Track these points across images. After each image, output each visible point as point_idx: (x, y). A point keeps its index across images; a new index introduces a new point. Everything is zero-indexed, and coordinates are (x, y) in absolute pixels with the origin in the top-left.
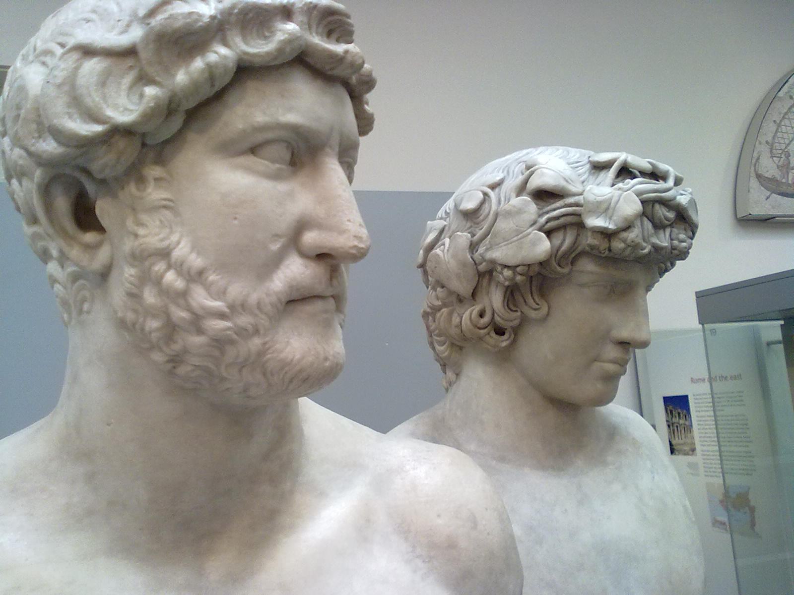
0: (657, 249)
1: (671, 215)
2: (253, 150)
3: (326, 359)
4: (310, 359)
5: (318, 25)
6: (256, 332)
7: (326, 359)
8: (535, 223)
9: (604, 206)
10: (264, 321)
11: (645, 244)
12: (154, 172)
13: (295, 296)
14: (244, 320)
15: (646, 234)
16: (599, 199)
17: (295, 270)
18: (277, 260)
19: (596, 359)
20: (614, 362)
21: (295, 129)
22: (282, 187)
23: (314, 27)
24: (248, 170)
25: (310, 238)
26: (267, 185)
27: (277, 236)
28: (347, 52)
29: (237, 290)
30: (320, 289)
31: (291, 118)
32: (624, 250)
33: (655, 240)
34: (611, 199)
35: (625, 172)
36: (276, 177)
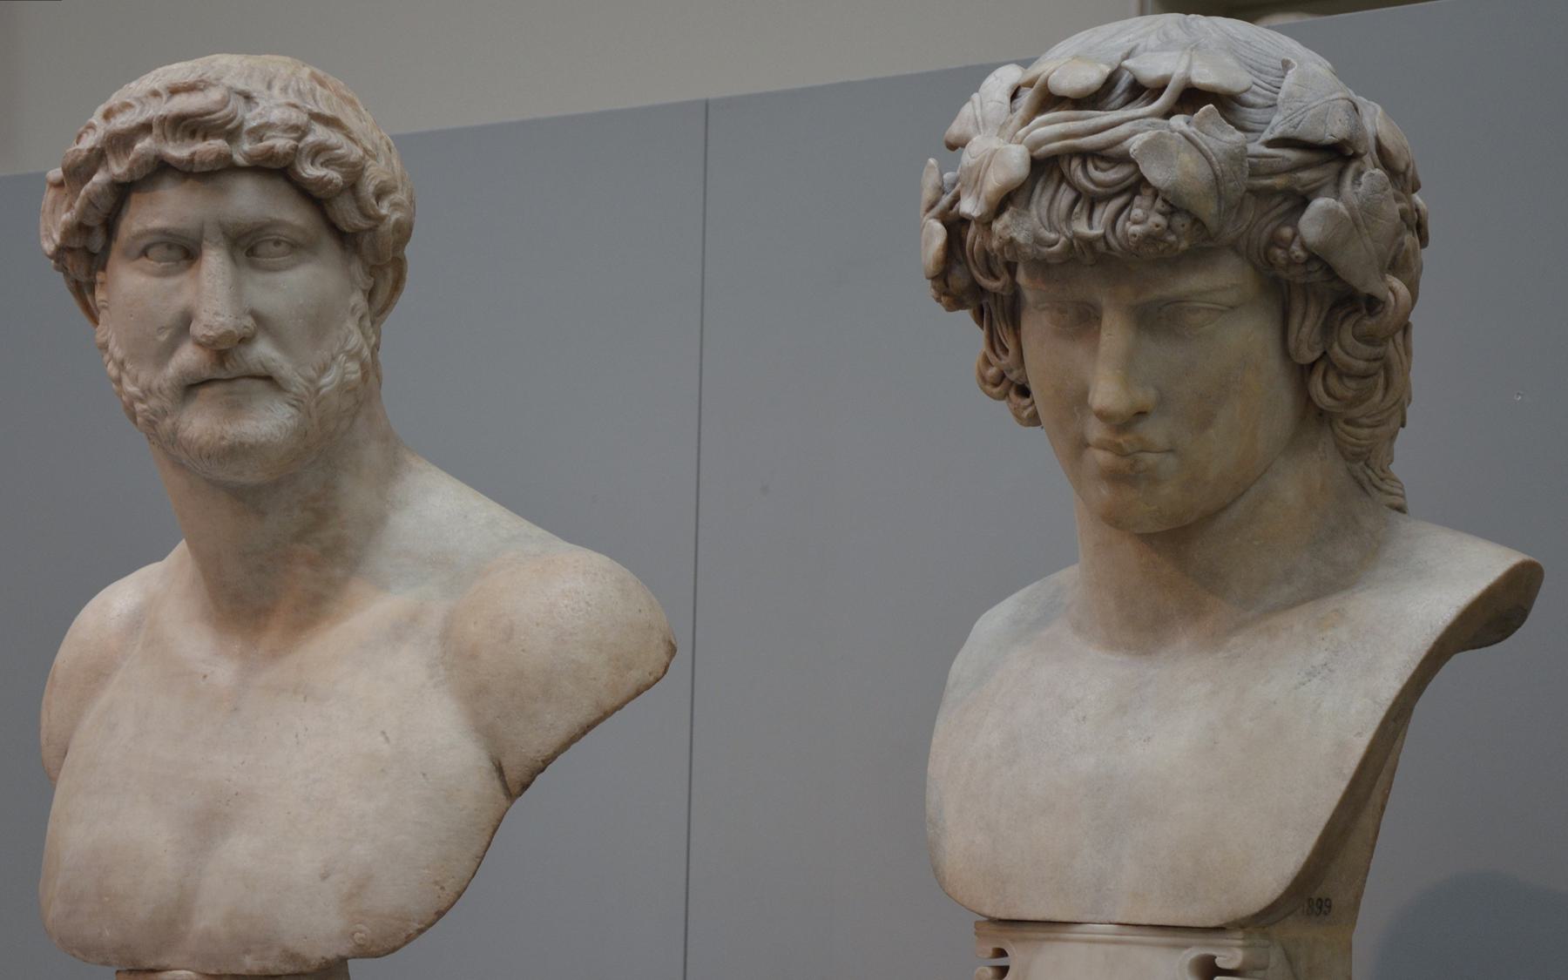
0: (1089, 243)
1: (1113, 175)
2: (144, 253)
3: (223, 438)
4: (206, 438)
5: (174, 134)
6: (165, 413)
7: (223, 438)
8: (932, 207)
9: (974, 176)
10: (168, 405)
11: (1053, 236)
12: (100, 277)
13: (189, 381)
14: (153, 403)
15: (1054, 218)
16: (972, 162)
17: (188, 357)
18: (171, 348)
19: (1082, 445)
20: (1102, 446)
21: (163, 232)
22: (171, 282)
23: (169, 135)
24: (142, 271)
25: (197, 329)
26: (155, 282)
27: (162, 329)
28: (193, 154)
29: (144, 377)
30: (206, 375)
31: (157, 223)
32: (1001, 250)
33: (1081, 227)
34: (981, 163)
35: (1049, 100)
36: (165, 274)
